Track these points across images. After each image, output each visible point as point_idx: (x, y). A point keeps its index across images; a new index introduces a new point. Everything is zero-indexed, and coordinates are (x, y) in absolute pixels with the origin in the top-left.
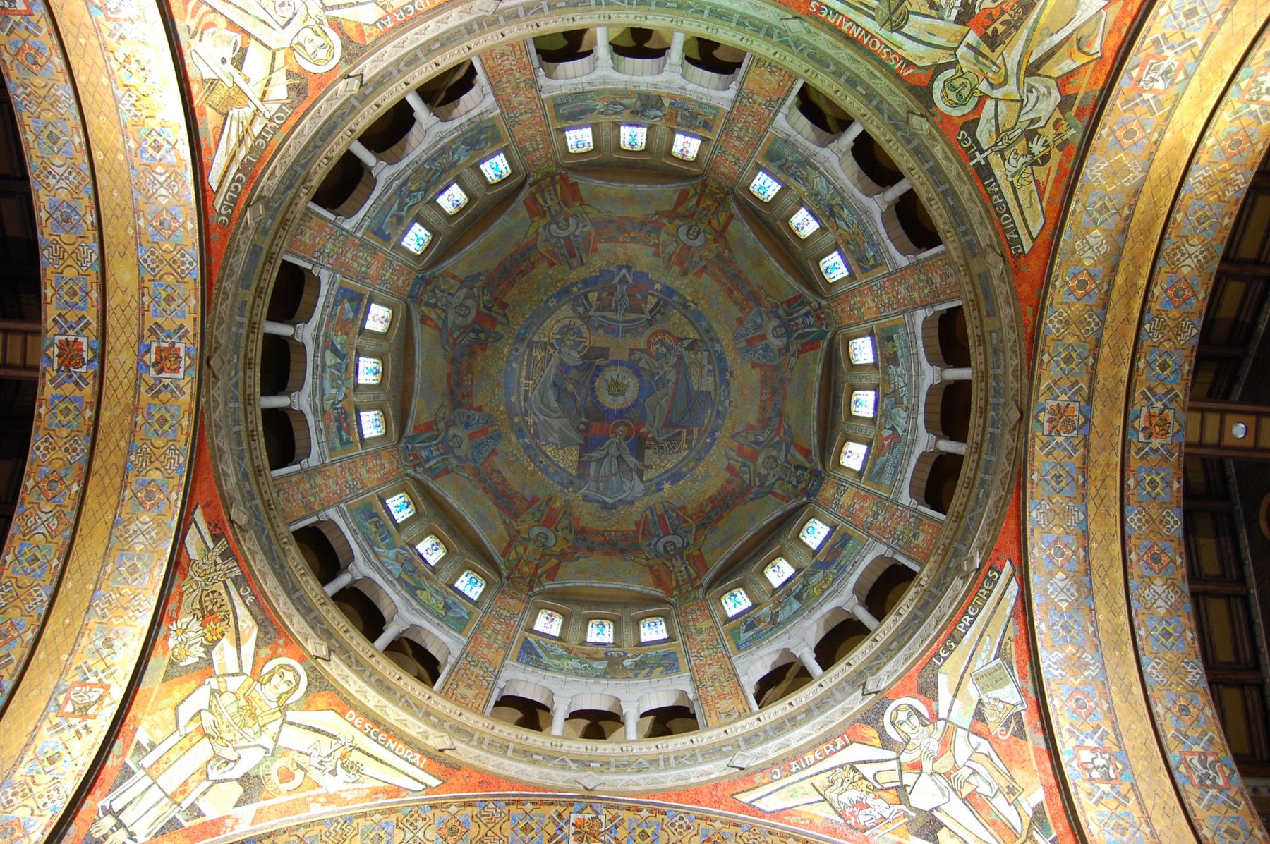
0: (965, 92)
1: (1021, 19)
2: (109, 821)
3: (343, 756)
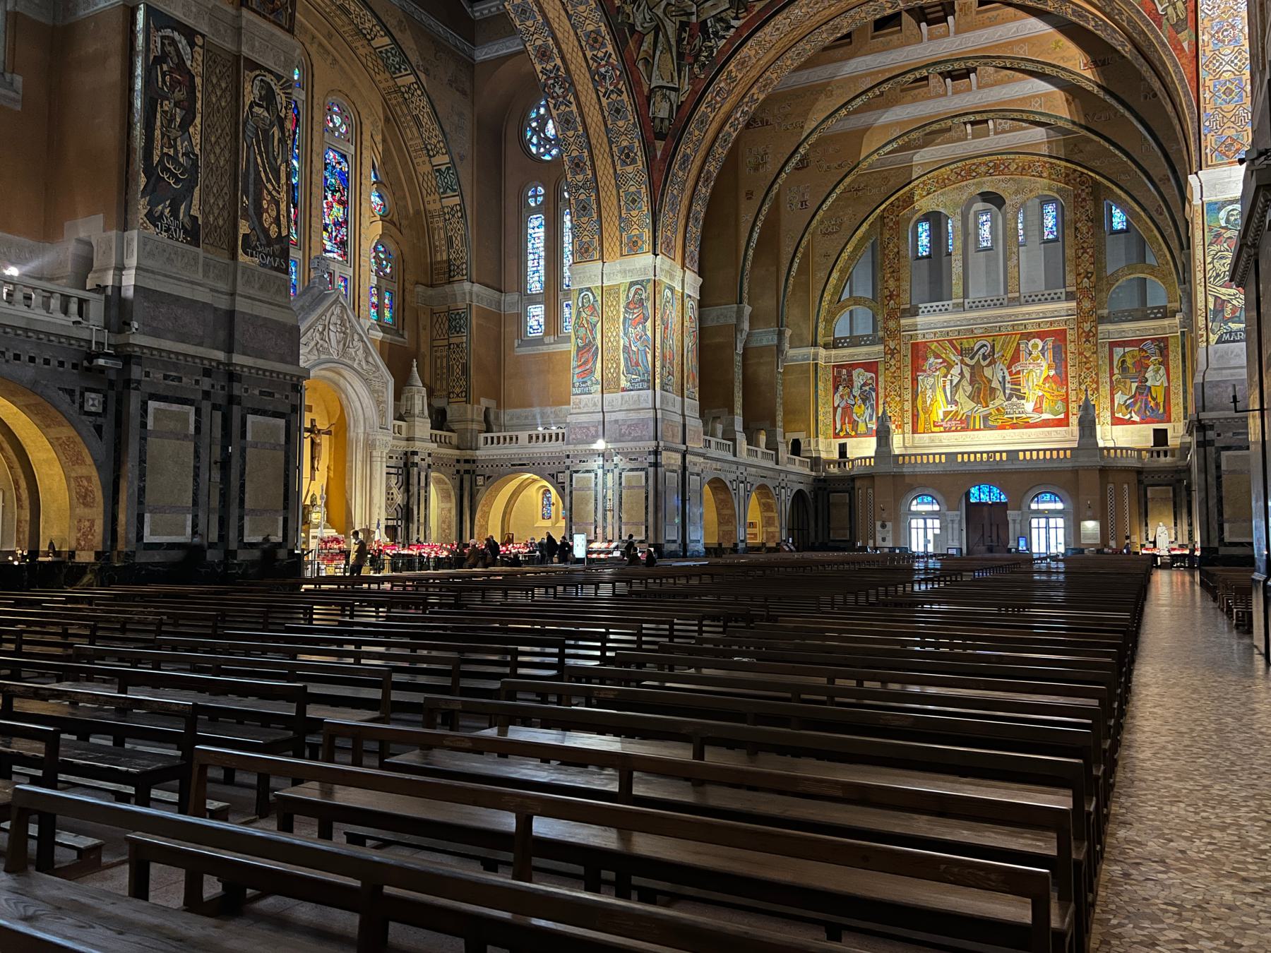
1: (678, 47)
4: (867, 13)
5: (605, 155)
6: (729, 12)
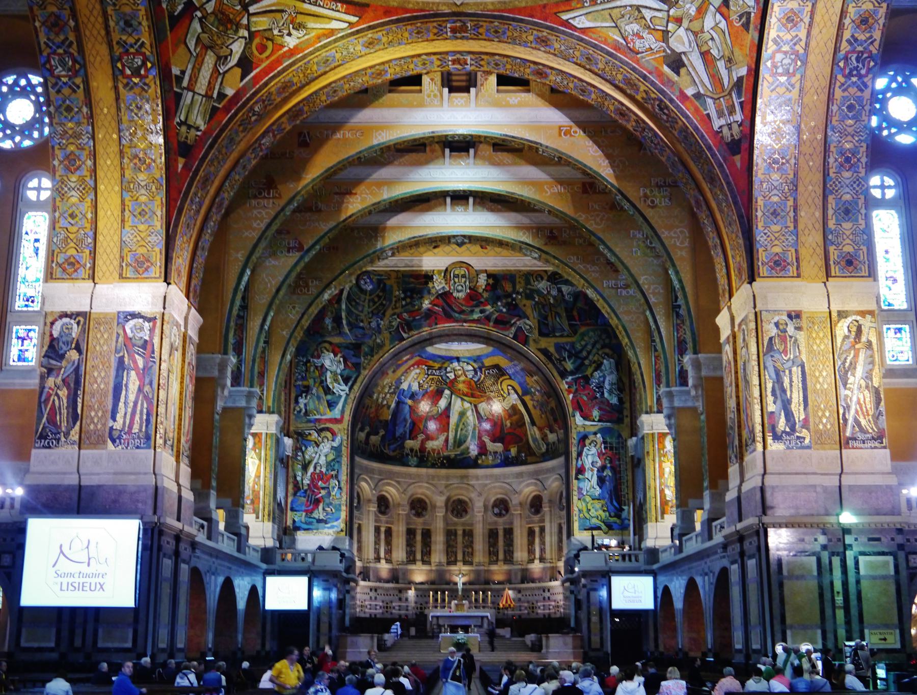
2: (184, 129)
3: (292, 22)
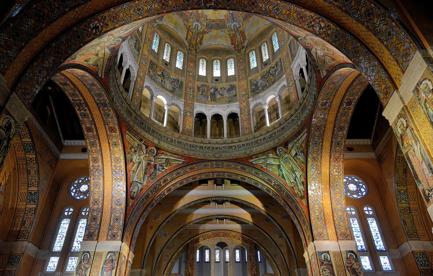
0: (150, 153)
4: (205, 176)
5: (109, 201)
6: (165, 164)
